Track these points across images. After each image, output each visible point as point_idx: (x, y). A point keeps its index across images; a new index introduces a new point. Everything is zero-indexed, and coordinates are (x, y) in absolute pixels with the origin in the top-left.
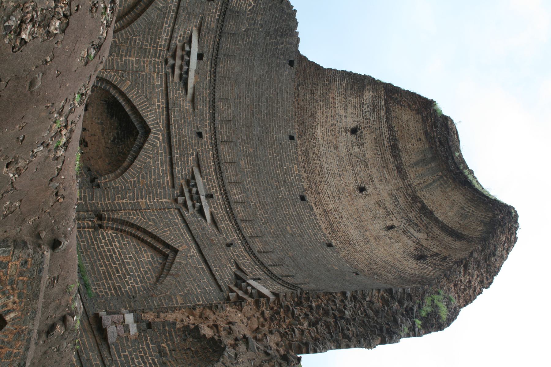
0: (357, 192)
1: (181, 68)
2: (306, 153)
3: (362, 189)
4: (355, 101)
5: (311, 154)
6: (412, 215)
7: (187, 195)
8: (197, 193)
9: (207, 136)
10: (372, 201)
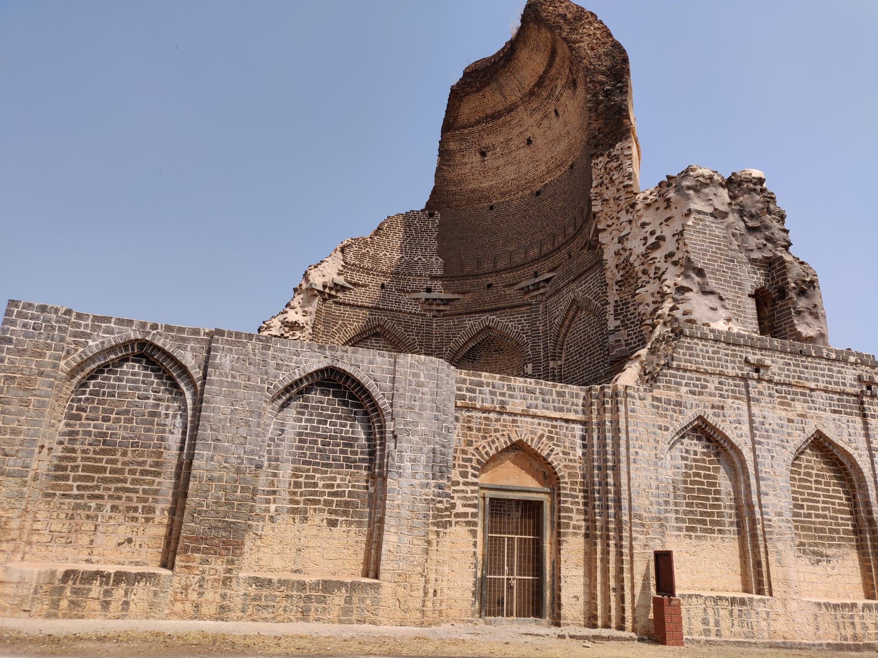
0: (532, 146)
1: (438, 305)
2: (503, 194)
3: (529, 142)
4: (458, 156)
5: (504, 190)
6: (545, 94)
7: (536, 293)
8: (533, 285)
10: (537, 132)
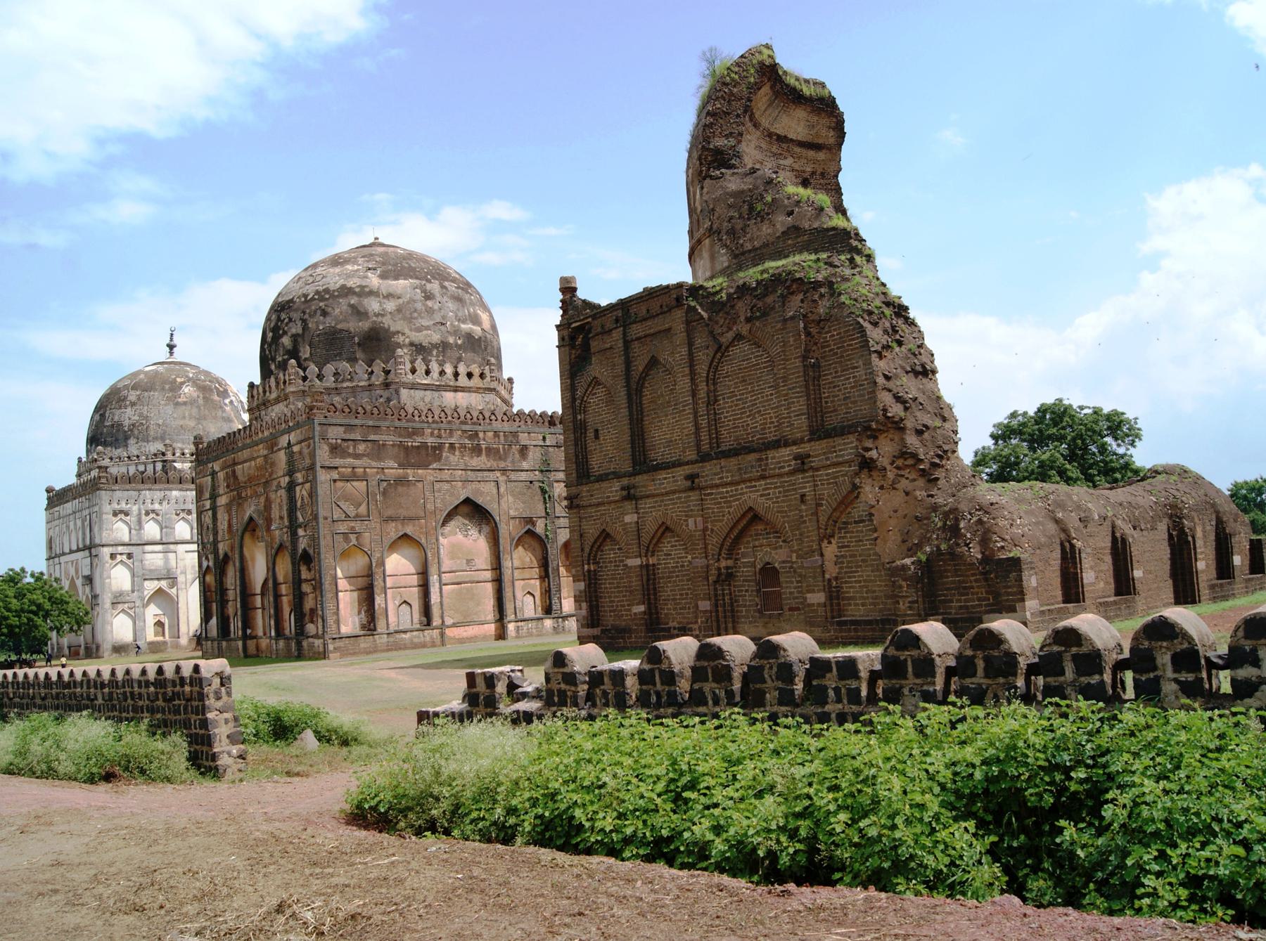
6: (774, 149)
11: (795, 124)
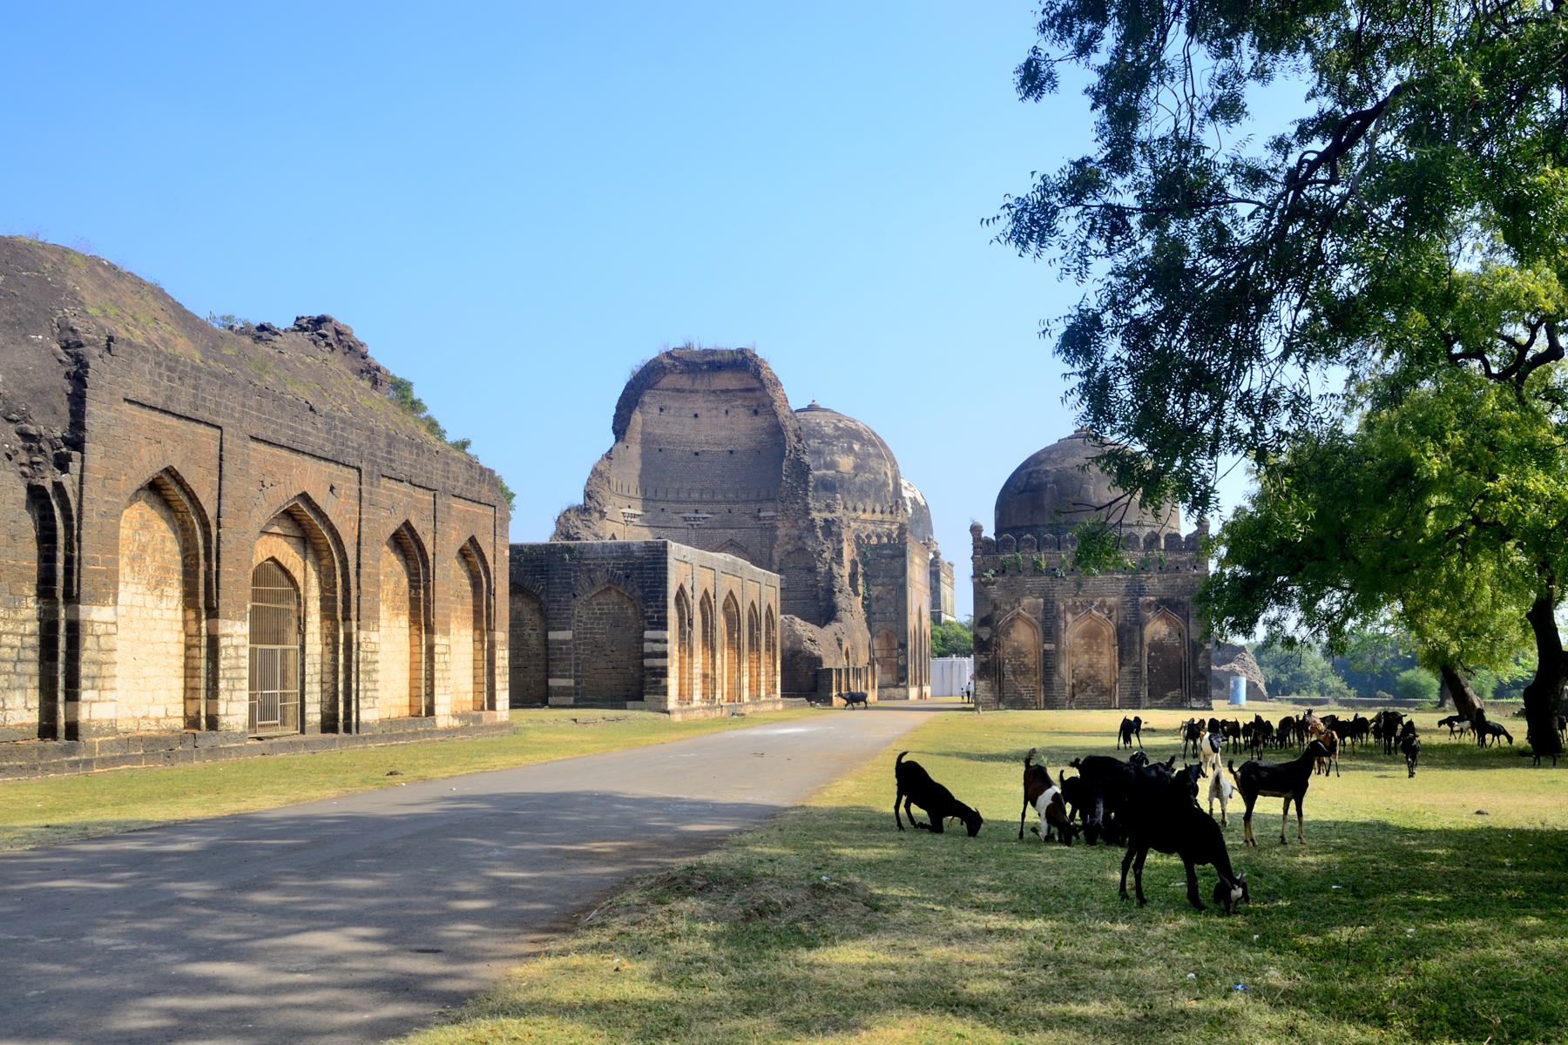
9: (663, 506)
10: (704, 413)
11: (726, 380)
